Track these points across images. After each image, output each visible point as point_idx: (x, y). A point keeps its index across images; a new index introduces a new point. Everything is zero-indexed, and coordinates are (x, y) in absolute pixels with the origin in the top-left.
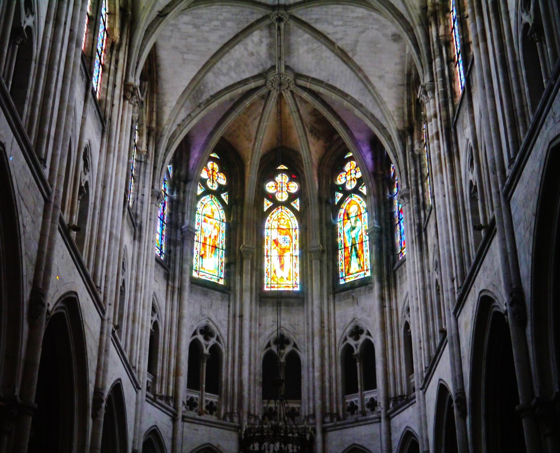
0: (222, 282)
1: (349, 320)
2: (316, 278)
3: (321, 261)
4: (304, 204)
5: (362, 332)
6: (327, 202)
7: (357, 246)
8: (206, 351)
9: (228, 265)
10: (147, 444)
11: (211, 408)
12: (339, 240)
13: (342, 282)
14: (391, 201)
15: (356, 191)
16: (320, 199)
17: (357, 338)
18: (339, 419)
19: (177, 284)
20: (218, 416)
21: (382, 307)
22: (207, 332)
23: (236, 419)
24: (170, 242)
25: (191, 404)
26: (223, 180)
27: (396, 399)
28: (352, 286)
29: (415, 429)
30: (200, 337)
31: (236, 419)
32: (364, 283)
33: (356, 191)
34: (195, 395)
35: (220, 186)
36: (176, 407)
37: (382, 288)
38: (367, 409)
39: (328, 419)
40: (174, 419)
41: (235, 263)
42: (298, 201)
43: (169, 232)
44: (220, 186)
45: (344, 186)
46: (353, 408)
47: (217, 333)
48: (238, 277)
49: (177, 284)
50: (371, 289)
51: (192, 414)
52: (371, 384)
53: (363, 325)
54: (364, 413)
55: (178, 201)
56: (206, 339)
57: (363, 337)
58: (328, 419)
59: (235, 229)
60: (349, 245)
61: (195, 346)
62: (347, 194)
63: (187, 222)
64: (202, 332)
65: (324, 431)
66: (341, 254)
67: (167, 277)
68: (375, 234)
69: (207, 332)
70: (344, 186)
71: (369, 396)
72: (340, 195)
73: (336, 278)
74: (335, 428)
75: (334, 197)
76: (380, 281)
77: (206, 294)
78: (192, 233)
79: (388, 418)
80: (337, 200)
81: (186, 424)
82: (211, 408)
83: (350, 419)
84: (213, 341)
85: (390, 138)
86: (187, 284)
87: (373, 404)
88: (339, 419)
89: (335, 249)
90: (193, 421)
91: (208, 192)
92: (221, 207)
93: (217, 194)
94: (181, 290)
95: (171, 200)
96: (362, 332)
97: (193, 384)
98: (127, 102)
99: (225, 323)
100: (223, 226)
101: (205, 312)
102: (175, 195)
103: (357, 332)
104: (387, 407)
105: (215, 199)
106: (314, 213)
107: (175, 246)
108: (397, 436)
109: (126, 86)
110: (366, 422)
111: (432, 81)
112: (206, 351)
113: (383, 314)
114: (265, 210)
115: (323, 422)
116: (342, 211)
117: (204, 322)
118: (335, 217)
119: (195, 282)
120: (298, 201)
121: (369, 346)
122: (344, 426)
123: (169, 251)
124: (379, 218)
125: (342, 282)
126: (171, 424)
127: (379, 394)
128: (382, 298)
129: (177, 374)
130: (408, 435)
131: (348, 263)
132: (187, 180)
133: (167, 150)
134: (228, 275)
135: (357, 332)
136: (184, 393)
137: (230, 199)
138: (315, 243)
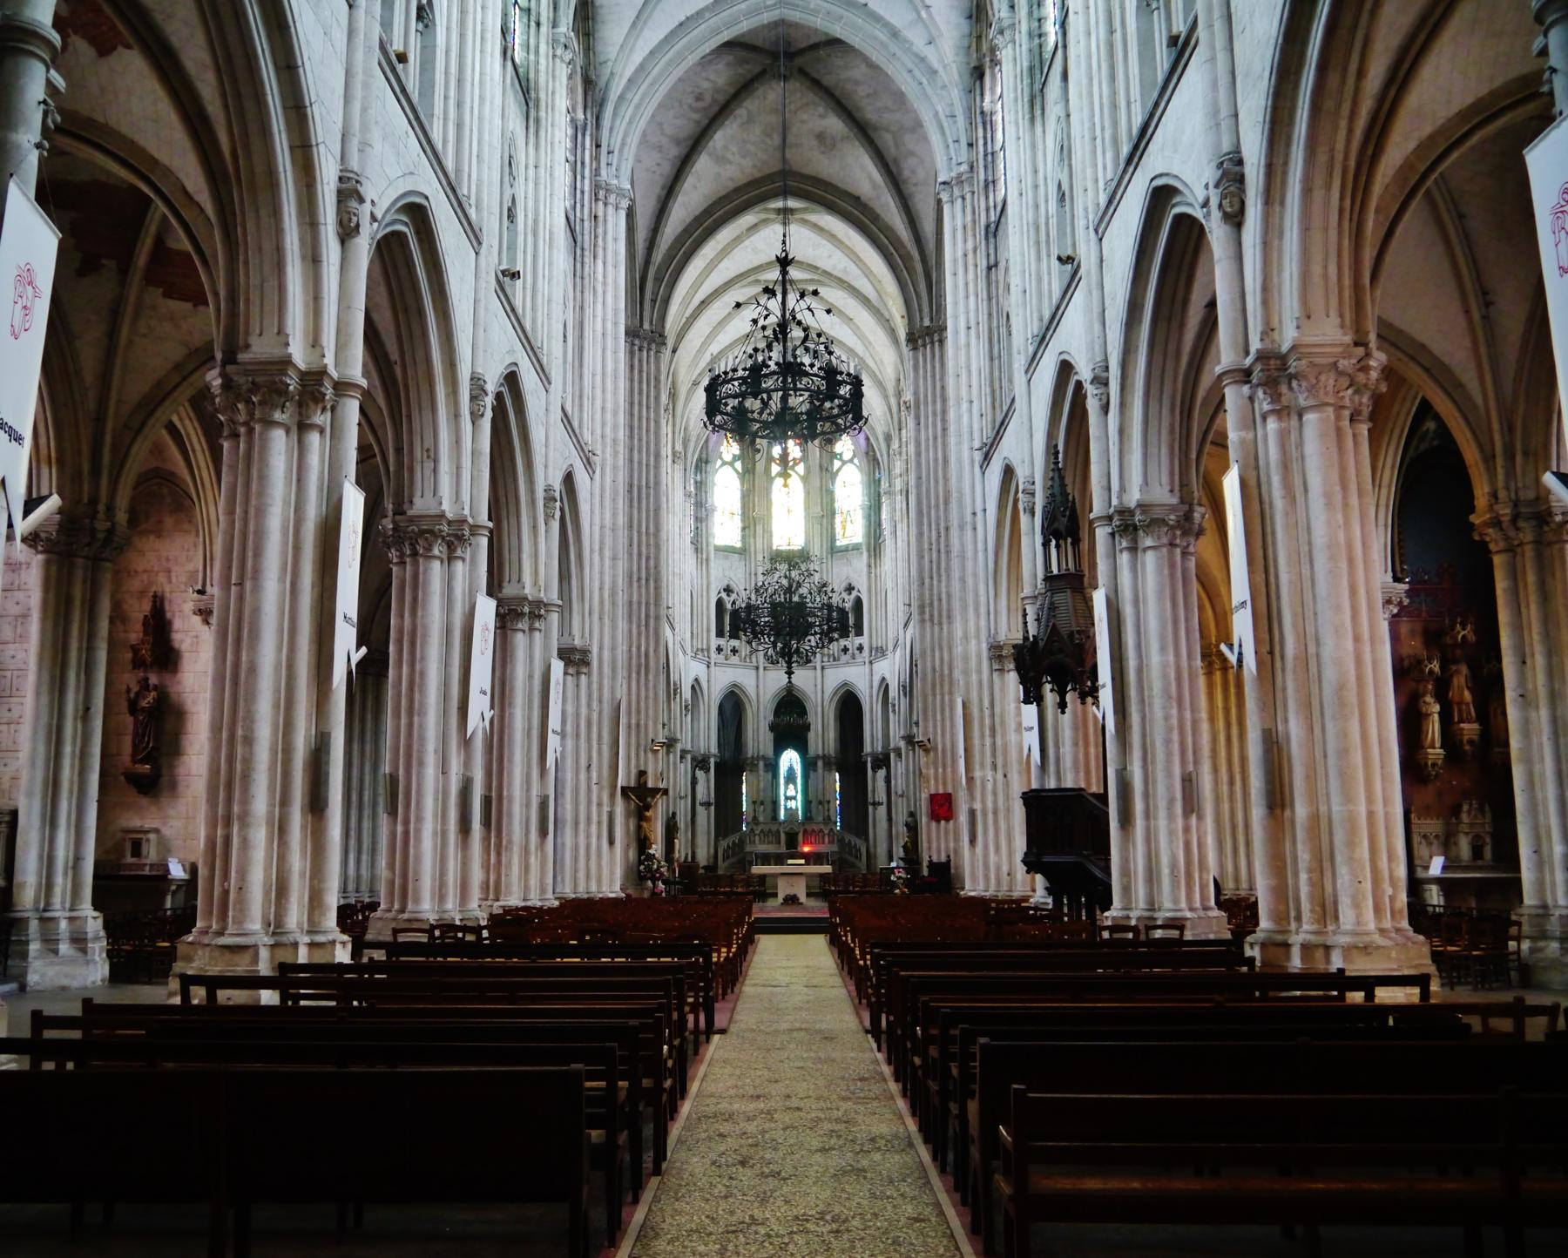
0: (739, 545)
2: (817, 540)
4: (808, 470)
9: (743, 529)
10: (693, 687)
11: (734, 651)
12: (836, 505)
13: (838, 543)
14: (879, 480)
15: (851, 461)
16: (821, 467)
18: (834, 660)
22: (728, 590)
23: (754, 659)
24: (697, 519)
25: (719, 650)
28: (846, 549)
29: (887, 676)
30: (724, 595)
32: (856, 547)
33: (851, 461)
34: (722, 642)
35: (734, 456)
37: (869, 556)
38: (857, 652)
39: (826, 659)
42: (802, 465)
44: (734, 456)
45: (841, 455)
46: (845, 650)
47: (736, 590)
51: (721, 658)
52: (859, 633)
53: (853, 584)
57: (854, 593)
58: (826, 659)
60: (845, 512)
61: (720, 603)
62: (844, 463)
65: (823, 668)
66: (838, 519)
67: (697, 549)
69: (728, 590)
70: (841, 455)
71: (858, 641)
72: (837, 464)
73: (833, 539)
74: (832, 666)
75: (832, 464)
76: (869, 551)
77: (727, 558)
79: (871, 662)
80: (835, 468)
83: (844, 658)
84: (733, 596)
88: (834, 660)
89: (833, 513)
91: (724, 463)
92: (735, 475)
93: (731, 464)
94: (707, 560)
95: (696, 482)
97: (720, 634)
98: (558, 61)
100: (738, 495)
101: (727, 573)
102: (698, 478)
103: (850, 589)
105: (730, 468)
106: (816, 482)
108: (876, 680)
112: (729, 606)
113: (869, 578)
116: (839, 480)
117: (726, 583)
118: (833, 484)
119: (718, 549)
120: (802, 465)
121: (858, 602)
124: (869, 495)
125: (838, 543)
127: (864, 640)
129: (708, 631)
130: (883, 679)
131: (844, 528)
132: (707, 462)
133: (694, 451)
134: (744, 537)
135: (850, 589)
136: (715, 642)
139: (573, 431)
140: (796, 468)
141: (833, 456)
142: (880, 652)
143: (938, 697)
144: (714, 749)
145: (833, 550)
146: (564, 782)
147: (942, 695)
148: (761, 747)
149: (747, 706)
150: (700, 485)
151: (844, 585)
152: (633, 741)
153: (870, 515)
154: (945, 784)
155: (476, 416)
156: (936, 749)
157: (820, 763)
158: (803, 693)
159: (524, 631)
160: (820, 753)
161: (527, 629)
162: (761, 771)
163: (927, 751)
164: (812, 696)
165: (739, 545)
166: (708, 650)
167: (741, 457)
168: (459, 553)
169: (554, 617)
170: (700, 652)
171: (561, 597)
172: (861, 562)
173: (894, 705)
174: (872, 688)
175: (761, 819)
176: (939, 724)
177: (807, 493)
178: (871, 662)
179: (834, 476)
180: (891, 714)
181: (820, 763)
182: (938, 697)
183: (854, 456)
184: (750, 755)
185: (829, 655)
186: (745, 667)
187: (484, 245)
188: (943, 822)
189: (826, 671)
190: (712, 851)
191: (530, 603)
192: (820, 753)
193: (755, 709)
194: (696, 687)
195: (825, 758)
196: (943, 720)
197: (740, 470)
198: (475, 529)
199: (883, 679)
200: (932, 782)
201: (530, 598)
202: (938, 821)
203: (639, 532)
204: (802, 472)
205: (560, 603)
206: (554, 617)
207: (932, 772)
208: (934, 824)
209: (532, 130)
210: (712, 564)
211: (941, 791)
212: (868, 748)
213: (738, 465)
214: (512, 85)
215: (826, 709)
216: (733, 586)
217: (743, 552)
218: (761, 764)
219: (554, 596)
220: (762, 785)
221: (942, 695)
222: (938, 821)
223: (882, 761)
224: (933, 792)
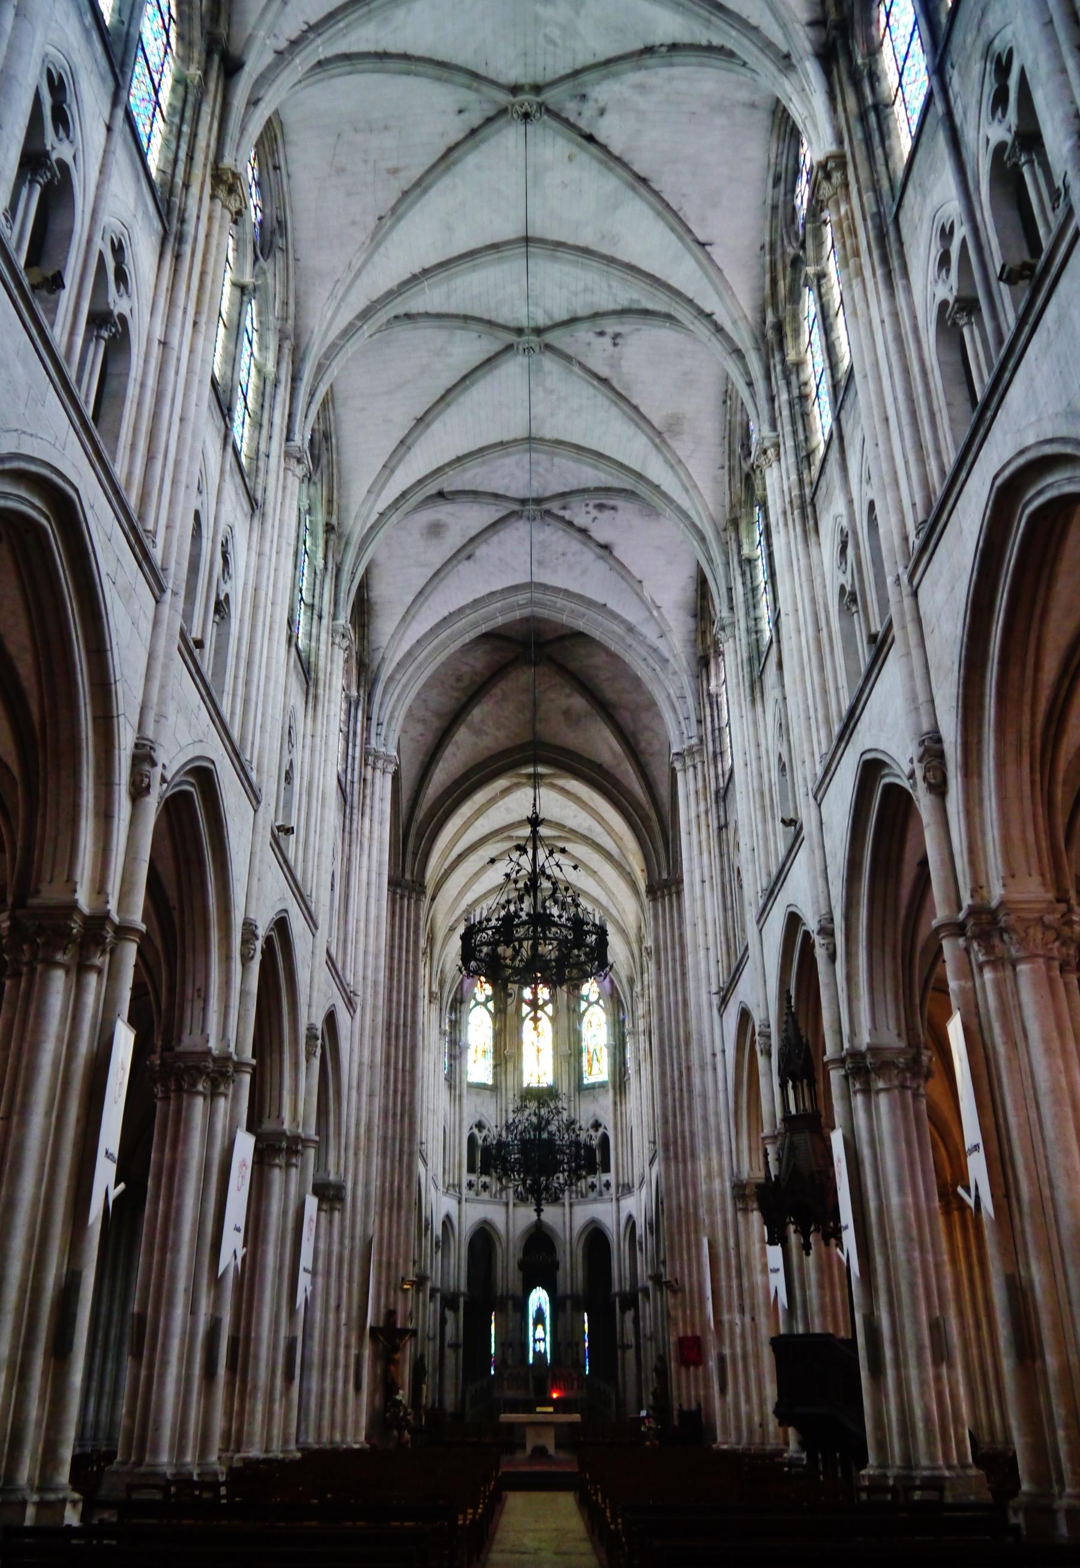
0: (490, 1082)
1: (591, 1114)
3: (569, 1063)
4: (556, 1010)
5: (600, 1125)
6: (574, 1010)
7: (598, 1052)
8: (480, 1142)
9: (495, 1066)
10: (444, 1223)
11: (485, 1187)
12: (584, 1044)
13: (586, 1082)
14: (624, 1020)
15: (597, 1002)
17: (597, 1130)
18: (582, 1196)
19: (457, 1093)
20: (491, 1193)
21: (615, 1110)
22: (480, 1126)
23: (504, 1196)
25: (470, 1185)
26: (488, 990)
27: (623, 1185)
28: (593, 1087)
29: (634, 1214)
30: (475, 1131)
31: (504, 1196)
32: (602, 1085)
33: (597, 1002)
34: (473, 1178)
35: (487, 997)
36: (460, 1193)
38: (604, 1189)
39: (574, 1196)
40: (460, 1203)
41: (500, 1065)
43: (450, 1049)
44: (487, 997)
45: (587, 996)
46: (593, 1186)
47: (487, 1125)
48: (503, 1077)
49: (457, 1093)
50: (608, 1091)
52: (606, 1169)
53: (601, 1120)
54: (601, 1194)
55: (456, 1021)
56: (480, 1131)
57: (601, 1130)
58: (574, 1196)
59: (500, 1034)
60: (591, 1050)
61: (472, 1139)
62: (590, 1004)
63: (463, 1038)
64: (477, 1126)
65: (571, 1205)
67: (450, 1087)
68: (612, 1049)
69: (480, 1126)
71: (605, 1177)
72: (584, 1005)
74: (579, 1203)
76: (614, 1089)
77: (478, 1094)
78: (467, 1047)
79: (618, 1200)
81: (468, 1204)
82: (485, 1187)
83: (592, 1195)
84: (485, 1132)
85: (621, 982)
86: (465, 1086)
87: (607, 1185)
88: (582, 1196)
90: (473, 1201)
91: (478, 1004)
93: (485, 1004)
94: (460, 1096)
95: (451, 1021)
96: (600, 1125)
97: (471, 1169)
98: (336, 647)
99: (494, 1116)
100: (490, 1033)
102: (453, 1017)
103: (597, 1125)
104: (617, 1192)
105: (483, 1009)
106: (563, 1021)
107: (455, 1059)
109: (431, 993)
110: (602, 1201)
111: (643, 989)
112: (480, 1142)
114: (524, 1015)
115: (571, 1198)
116: (586, 1019)
117: (477, 1119)
118: (580, 1023)
119: (471, 1086)
121: (605, 1138)
122: (586, 1203)
123: (451, 1065)
125: (586, 1082)
126: (457, 1205)
127: (611, 1177)
128: (615, 1103)
129: (460, 1166)
130: (630, 1217)
131: (591, 1066)
132: (461, 1002)
133: (450, 992)
135: (597, 1125)
136: (466, 1177)
137: (495, 1008)
138: (565, 1049)
139: (337, 972)
140: (546, 1009)
141: (580, 998)
142: (626, 1189)
143: (684, 1236)
144: (463, 1288)
145: (581, 1088)
146: (309, 1391)
147: (688, 1234)
148: (510, 1285)
149: (497, 1244)
150: (455, 1025)
151: (591, 1122)
152: (383, 1279)
153: (615, 1054)
154: (693, 1326)
155: (246, 959)
156: (683, 1290)
157: (569, 1304)
158: (551, 1229)
159: (280, 1167)
160: (569, 1292)
161: (283, 1165)
162: (510, 1312)
163: (675, 1292)
164: (560, 1232)
165: (490, 1082)
166: (460, 1186)
167: (494, 997)
168: (222, 1089)
169: (311, 1153)
170: (454, 1188)
171: (318, 1133)
172: (607, 1099)
173: (641, 1244)
174: (618, 1225)
175: (510, 1362)
176: (686, 1263)
177: (556, 1033)
178: (618, 1200)
179: (581, 1016)
180: (638, 1254)
181: (569, 1304)
182: (684, 1236)
183: (599, 998)
184: (499, 1293)
185: (577, 1192)
186: (494, 1203)
187: (263, 804)
188: (692, 1369)
189: (577, 1209)
190: (460, 1396)
191: (288, 1138)
192: (569, 1292)
193: (504, 1245)
194: (447, 1221)
195: (574, 1297)
196: (690, 1259)
197: (493, 1010)
198: (239, 1066)
199: (630, 1217)
200: (681, 1325)
201: (288, 1133)
202: (688, 1367)
203: (396, 1069)
204: (550, 1013)
205: (317, 1138)
206: (311, 1153)
207: (680, 1313)
208: (683, 1370)
209: (310, 705)
210: (465, 1100)
211: (689, 1334)
212: (616, 1288)
213: (491, 1005)
214: (295, 667)
215: (574, 1248)
216: (485, 1122)
217: (495, 1089)
218: (510, 1304)
219: (312, 1132)
220: (511, 1325)
221: (688, 1234)
222: (688, 1367)
223: (630, 1301)
224: (681, 1334)
